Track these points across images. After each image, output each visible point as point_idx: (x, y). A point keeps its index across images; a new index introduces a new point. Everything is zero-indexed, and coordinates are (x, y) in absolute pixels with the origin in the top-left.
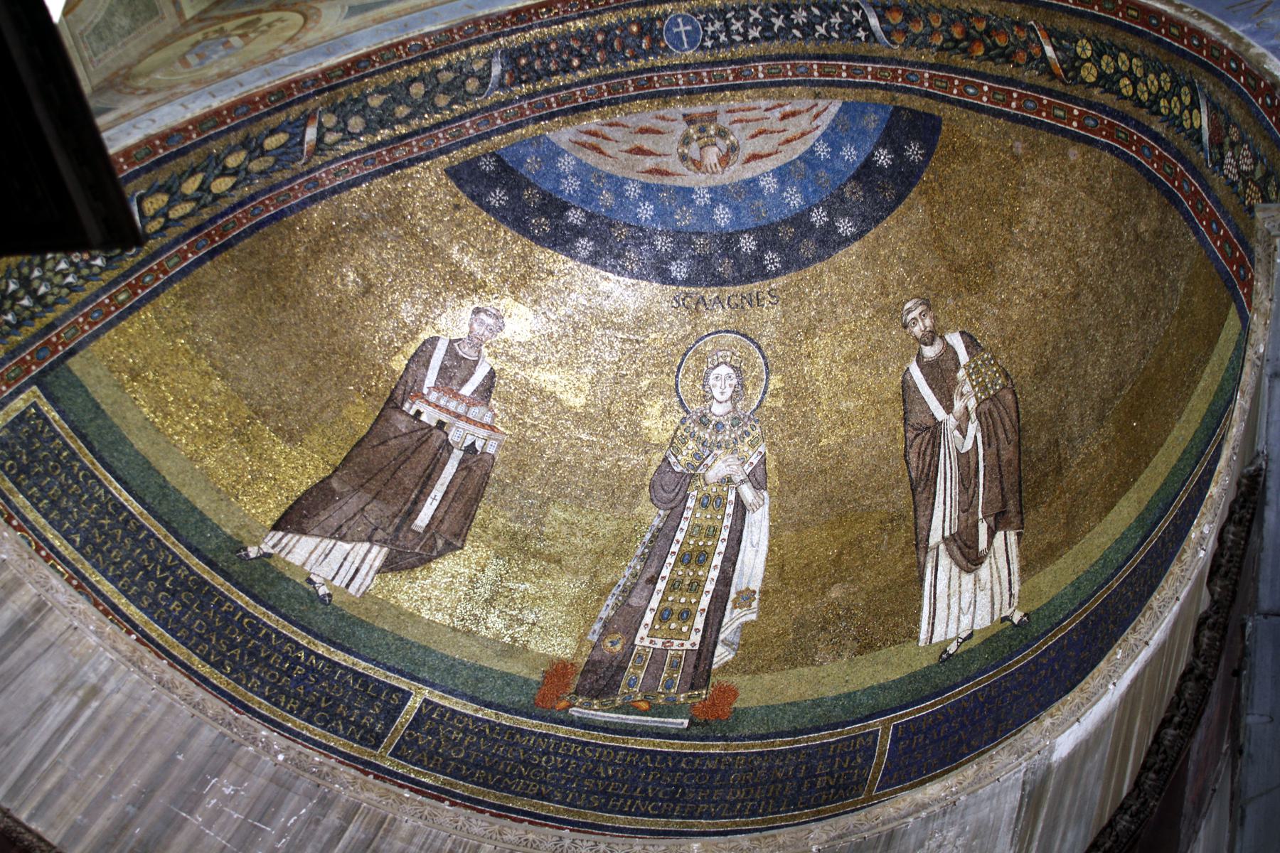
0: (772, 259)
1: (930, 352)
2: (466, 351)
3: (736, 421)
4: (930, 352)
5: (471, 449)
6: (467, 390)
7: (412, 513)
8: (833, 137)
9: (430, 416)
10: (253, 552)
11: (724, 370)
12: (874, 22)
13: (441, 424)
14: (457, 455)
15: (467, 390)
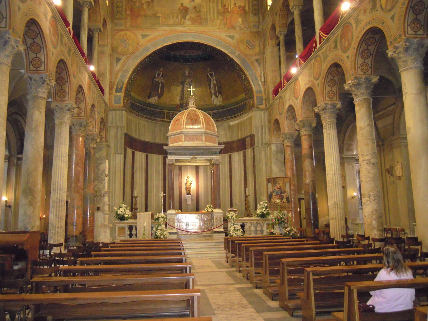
0: (193, 61)
1: (210, 73)
2: (159, 72)
3: (189, 76)
4: (210, 73)
5: (162, 82)
6: (160, 76)
7: (158, 92)
8: (202, 54)
9: (157, 80)
10: (147, 102)
11: (187, 71)
12: (209, 49)
13: (158, 80)
14: (160, 83)
15: (160, 76)
